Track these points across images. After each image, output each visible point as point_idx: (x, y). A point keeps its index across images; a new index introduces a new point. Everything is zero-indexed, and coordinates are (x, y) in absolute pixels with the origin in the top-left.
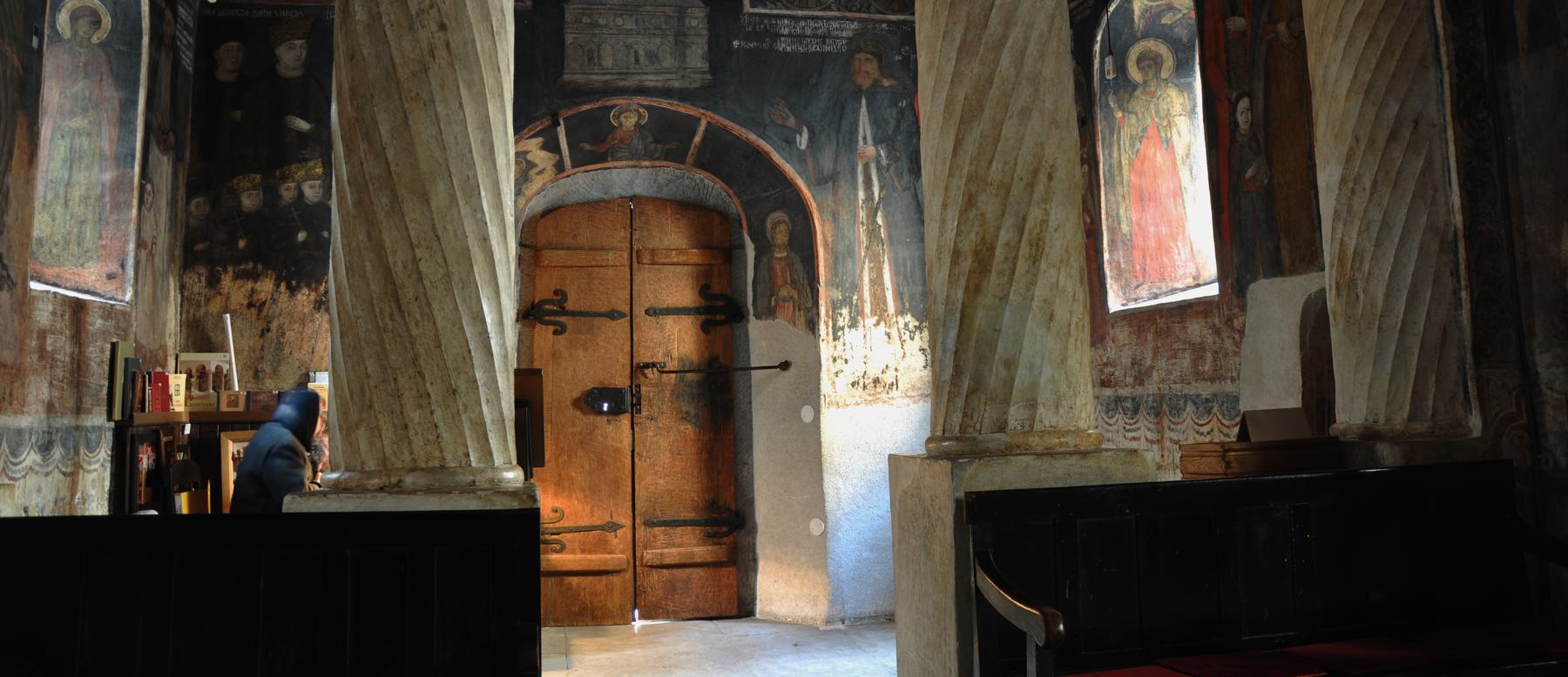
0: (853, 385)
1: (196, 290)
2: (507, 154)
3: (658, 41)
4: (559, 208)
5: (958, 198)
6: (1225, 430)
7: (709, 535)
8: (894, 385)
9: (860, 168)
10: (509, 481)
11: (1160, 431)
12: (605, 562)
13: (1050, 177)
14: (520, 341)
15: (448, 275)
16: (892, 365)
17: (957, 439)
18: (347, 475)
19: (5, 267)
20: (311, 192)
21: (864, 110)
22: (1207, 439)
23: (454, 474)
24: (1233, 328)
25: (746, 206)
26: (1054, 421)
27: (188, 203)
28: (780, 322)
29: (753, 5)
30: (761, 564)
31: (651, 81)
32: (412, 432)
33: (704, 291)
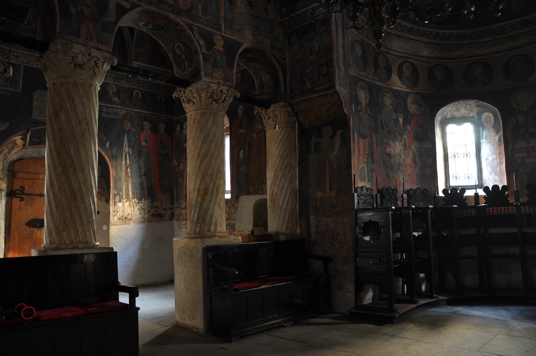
4: (23, 159)
9: (124, 155)
16: (130, 213)
21: (126, 137)
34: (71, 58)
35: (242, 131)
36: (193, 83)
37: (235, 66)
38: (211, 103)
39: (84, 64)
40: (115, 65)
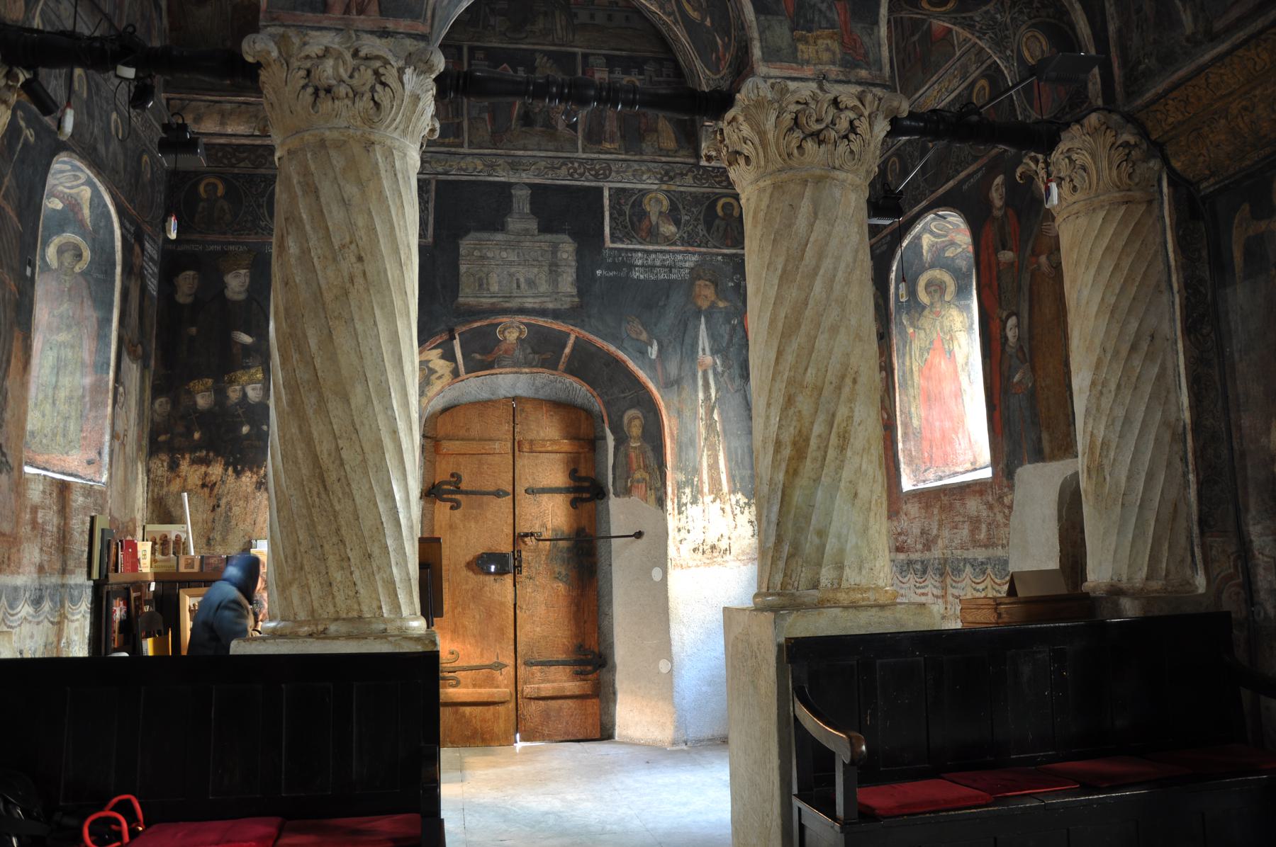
0: (694, 550)
1: (159, 473)
2: (413, 363)
3: (536, 270)
5: (779, 399)
6: (997, 588)
7: (577, 673)
8: (727, 551)
9: (700, 374)
10: (414, 629)
11: (944, 588)
12: (492, 695)
13: (855, 381)
14: (423, 515)
15: (364, 461)
17: (779, 594)
18: (282, 624)
19: (4, 455)
20: (253, 394)
21: (703, 326)
22: (983, 595)
23: (370, 623)
24: (1003, 504)
25: (607, 404)
26: (857, 581)
27: (152, 403)
28: (635, 499)
29: (613, 242)
30: (619, 697)
31: (530, 303)
32: (335, 589)
33: (573, 474)
34: (303, 73)
35: (1007, 256)
38: (800, 147)
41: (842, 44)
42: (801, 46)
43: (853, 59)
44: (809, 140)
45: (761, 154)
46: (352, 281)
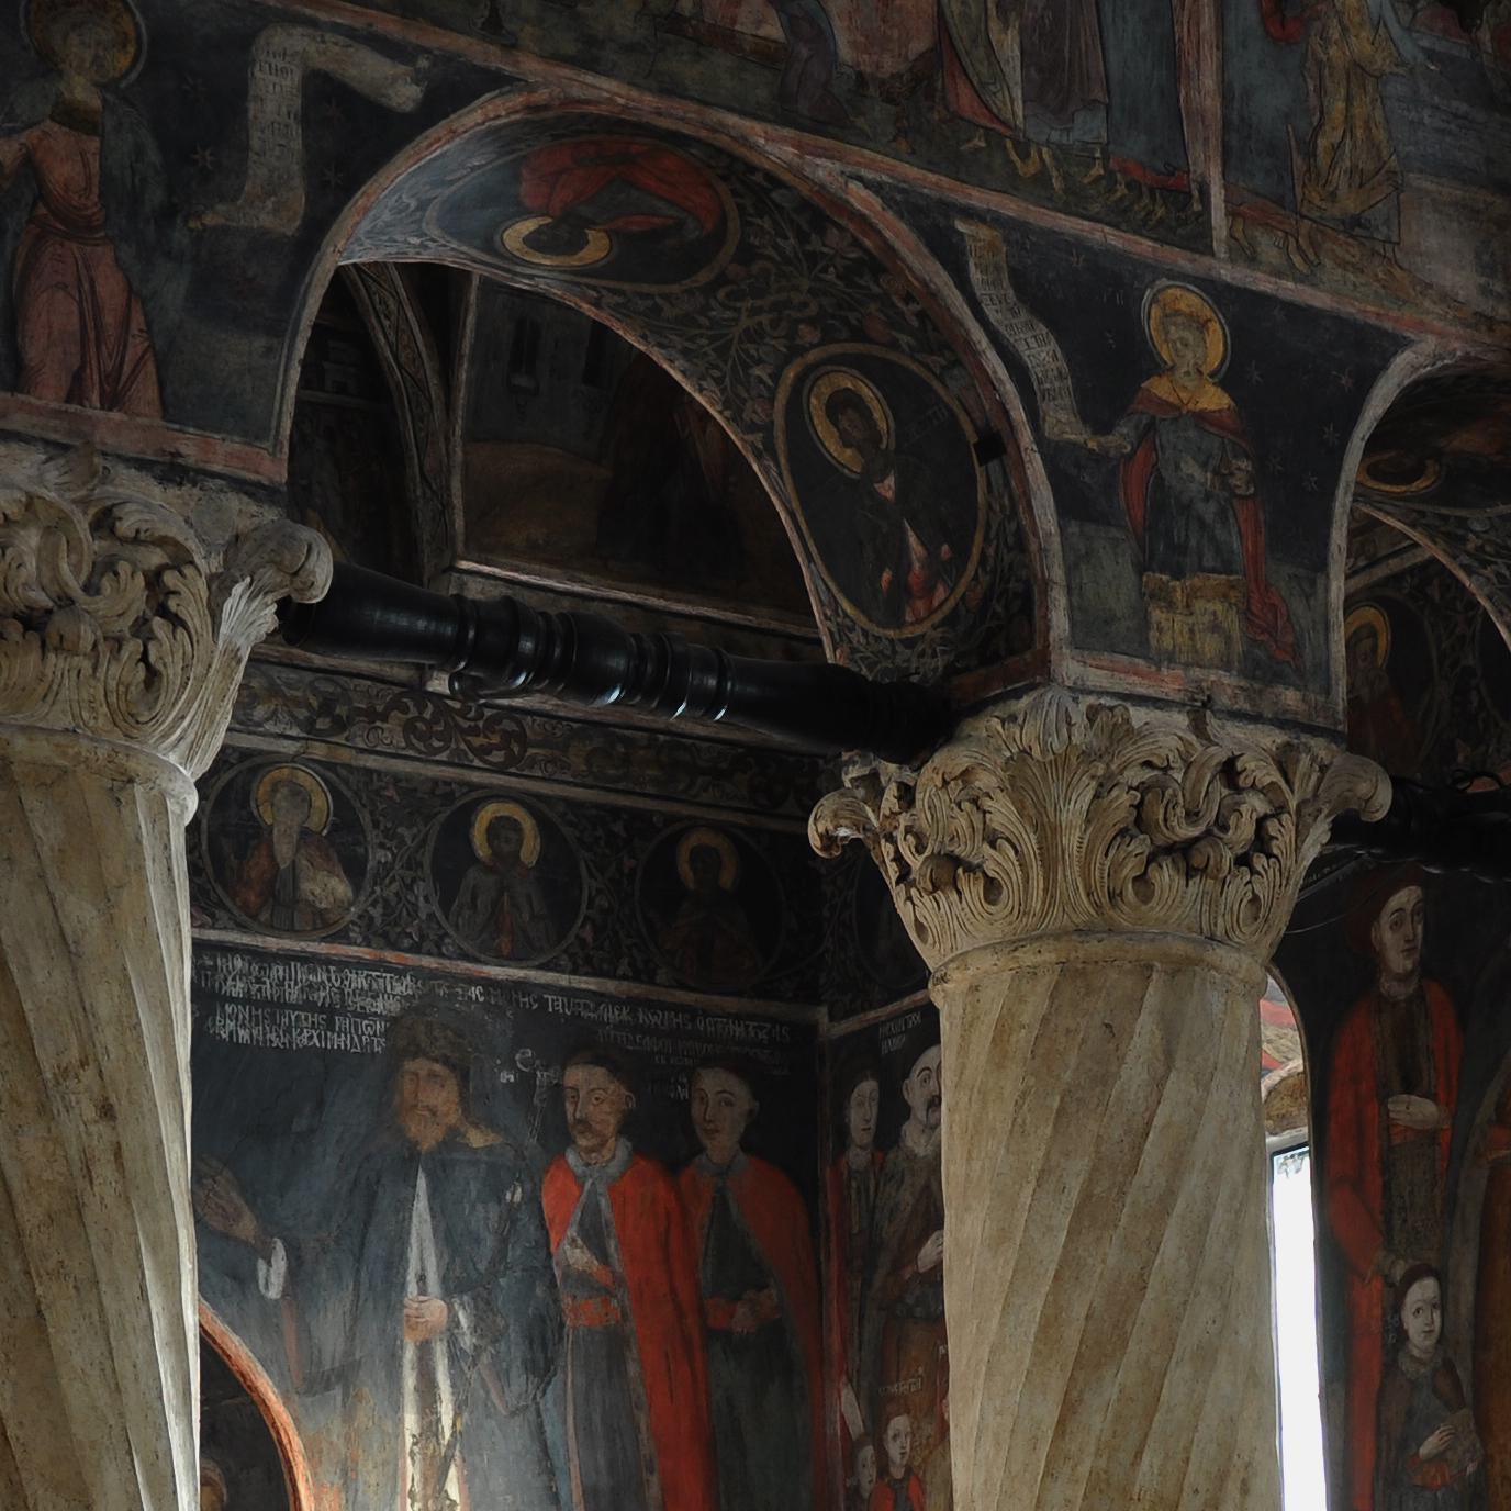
21: (421, 1205)
36: (977, 708)
37: (1339, 537)
38: (1141, 880)
39: (65, 601)
40: (318, 595)
41: (1247, 615)
42: (1157, 615)
43: (1270, 658)
44: (1166, 863)
45: (1038, 883)
46: (89, 1175)
